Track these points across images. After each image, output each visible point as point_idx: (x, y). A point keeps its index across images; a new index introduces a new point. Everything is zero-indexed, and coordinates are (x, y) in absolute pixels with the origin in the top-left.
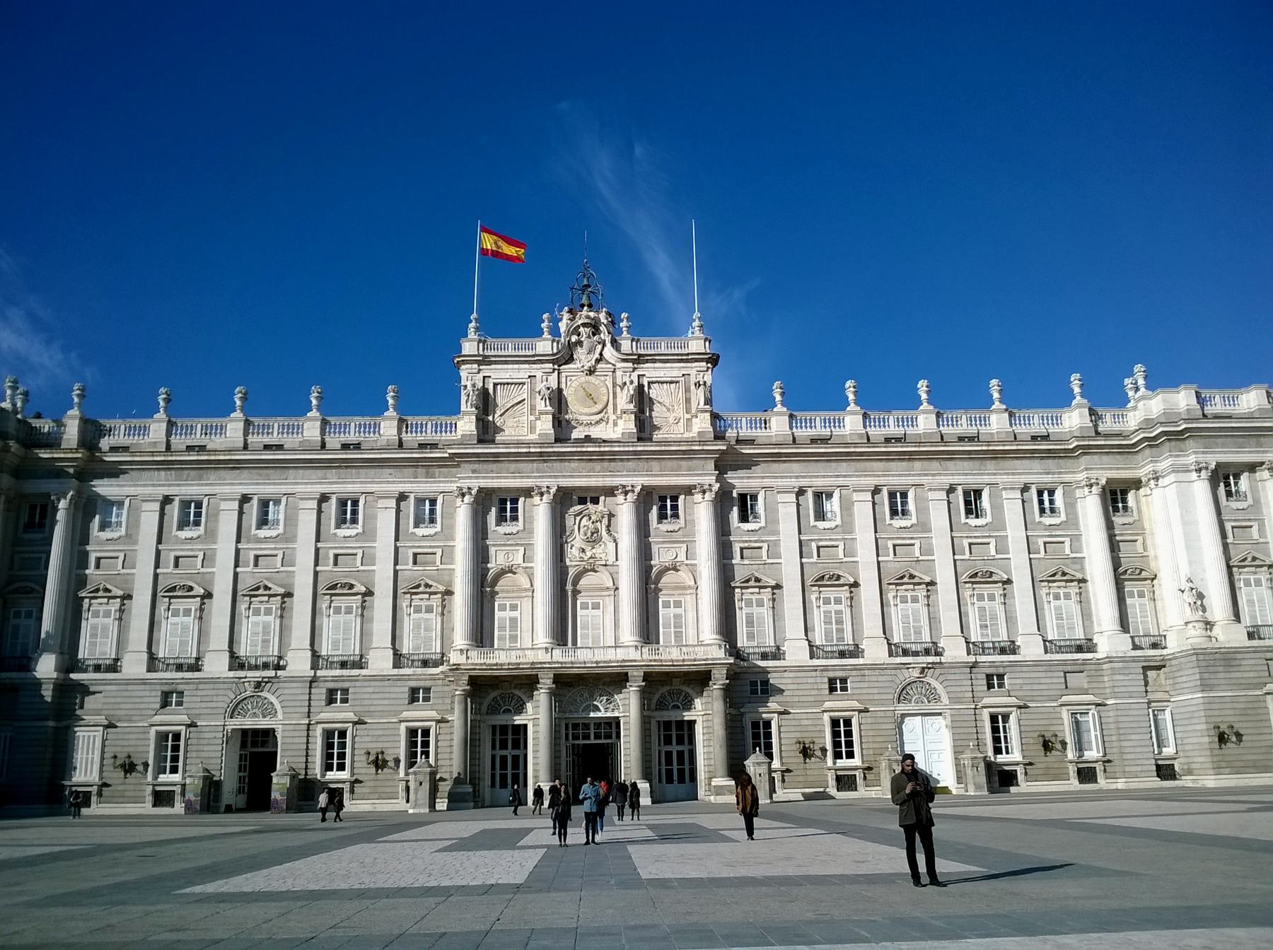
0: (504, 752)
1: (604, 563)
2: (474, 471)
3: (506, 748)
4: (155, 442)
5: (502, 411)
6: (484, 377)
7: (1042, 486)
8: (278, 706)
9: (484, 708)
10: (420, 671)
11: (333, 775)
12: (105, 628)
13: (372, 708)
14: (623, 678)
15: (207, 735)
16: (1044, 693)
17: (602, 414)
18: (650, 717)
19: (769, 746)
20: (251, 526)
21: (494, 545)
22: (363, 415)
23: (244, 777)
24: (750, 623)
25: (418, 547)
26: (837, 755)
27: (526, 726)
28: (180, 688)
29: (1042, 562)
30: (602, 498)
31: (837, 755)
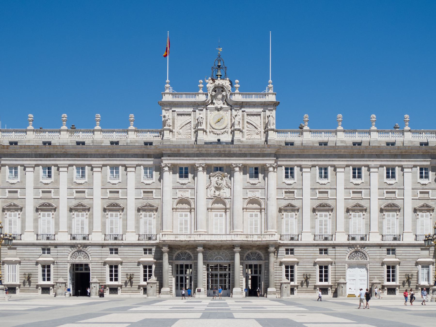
0: (182, 275)
1: (225, 197)
2: (169, 156)
4: (29, 140)
5: (181, 127)
7: (422, 167)
8: (89, 255)
9: (174, 257)
12: (15, 222)
13: (128, 257)
14: (232, 247)
16: (411, 257)
17: (225, 129)
18: (243, 263)
19: (292, 276)
20: (73, 178)
21: (178, 189)
24: (287, 224)
25: (145, 189)
26: (321, 280)
27: (191, 265)
29: (418, 200)
30: (225, 168)
31: (321, 280)
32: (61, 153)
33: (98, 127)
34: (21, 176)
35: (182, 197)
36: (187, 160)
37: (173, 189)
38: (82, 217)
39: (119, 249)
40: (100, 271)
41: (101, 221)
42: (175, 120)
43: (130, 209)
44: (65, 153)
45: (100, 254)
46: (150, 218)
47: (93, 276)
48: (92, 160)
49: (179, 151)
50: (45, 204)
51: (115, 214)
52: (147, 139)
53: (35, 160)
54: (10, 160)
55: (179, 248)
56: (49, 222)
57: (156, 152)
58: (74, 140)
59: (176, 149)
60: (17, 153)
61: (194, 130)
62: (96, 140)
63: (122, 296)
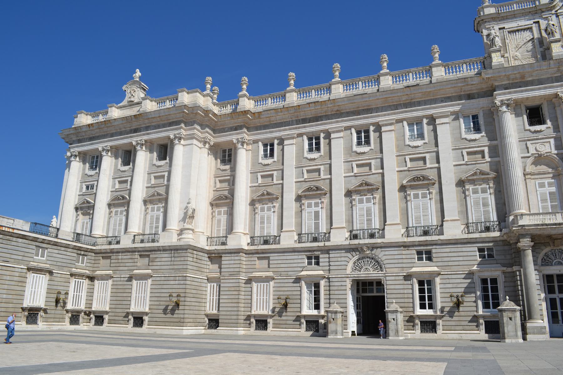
3: (554, 293)
5: (517, 49)
6: (500, 29)
10: (484, 235)
11: (428, 312)
12: (269, 218)
13: (450, 263)
15: (336, 284)
21: (529, 140)
22: (417, 66)
23: (360, 312)
25: (469, 148)
28: (317, 253)
32: (333, 113)
33: (385, 70)
34: (277, 153)
35: (539, 153)
36: (540, 89)
37: (520, 141)
38: (367, 202)
39: (434, 251)
40: (402, 291)
41: (400, 206)
42: (506, 40)
43: (447, 182)
44: (338, 112)
45: (400, 261)
46: (484, 195)
47: (389, 301)
48: (379, 116)
49: (523, 77)
50: (310, 188)
51: (422, 194)
52: (464, 74)
53: (296, 128)
54: (263, 133)
55: (548, 243)
56: (317, 214)
57: (482, 88)
58: (353, 94)
59: (518, 76)
60: (273, 122)
61: (542, 49)
62: (383, 88)
63: (446, 337)
